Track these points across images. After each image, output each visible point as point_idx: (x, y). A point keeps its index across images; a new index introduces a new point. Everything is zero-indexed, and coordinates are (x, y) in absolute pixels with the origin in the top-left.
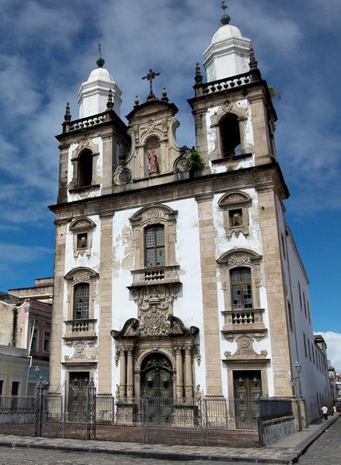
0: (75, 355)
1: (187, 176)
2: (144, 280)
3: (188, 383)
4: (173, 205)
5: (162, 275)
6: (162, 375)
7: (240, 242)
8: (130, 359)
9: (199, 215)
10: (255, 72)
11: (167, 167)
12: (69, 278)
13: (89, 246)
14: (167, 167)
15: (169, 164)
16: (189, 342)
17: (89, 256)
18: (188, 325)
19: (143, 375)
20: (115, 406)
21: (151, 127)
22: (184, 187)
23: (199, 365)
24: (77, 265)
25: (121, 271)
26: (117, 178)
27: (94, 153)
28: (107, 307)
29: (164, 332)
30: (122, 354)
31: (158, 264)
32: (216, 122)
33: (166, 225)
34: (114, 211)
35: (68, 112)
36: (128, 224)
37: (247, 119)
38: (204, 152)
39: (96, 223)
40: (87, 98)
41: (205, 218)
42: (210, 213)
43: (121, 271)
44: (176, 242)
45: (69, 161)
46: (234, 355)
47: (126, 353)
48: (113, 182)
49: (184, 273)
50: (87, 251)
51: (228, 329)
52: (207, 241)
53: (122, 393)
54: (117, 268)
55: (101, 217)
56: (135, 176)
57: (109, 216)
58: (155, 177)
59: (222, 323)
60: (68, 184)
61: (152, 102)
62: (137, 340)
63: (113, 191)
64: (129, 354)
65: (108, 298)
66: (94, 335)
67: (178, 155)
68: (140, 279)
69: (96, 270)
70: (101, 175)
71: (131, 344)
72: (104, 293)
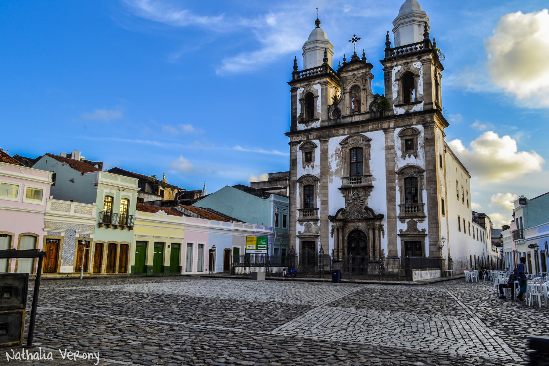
0: (305, 231)
1: (378, 115)
2: (349, 184)
3: (377, 247)
4: (368, 135)
5: (361, 181)
6: (361, 244)
7: (411, 161)
8: (340, 234)
10: (426, 41)
11: (365, 108)
13: (313, 161)
14: (365, 108)
15: (367, 106)
16: (377, 223)
17: (313, 167)
18: (377, 213)
19: (349, 243)
20: (331, 262)
21: (354, 79)
22: (375, 123)
23: (383, 237)
24: (305, 173)
25: (334, 177)
26: (331, 114)
27: (315, 96)
28: (325, 201)
29: (361, 217)
30: (336, 230)
31: (359, 173)
32: (398, 77)
33: (364, 148)
34: (329, 137)
35: (295, 63)
36: (340, 147)
37: (420, 76)
38: (390, 98)
39: (317, 145)
40: (309, 53)
41: (390, 144)
42: (392, 141)
43: (334, 177)
44: (370, 159)
45: (298, 100)
46: (406, 231)
47: (338, 230)
49: (375, 179)
50: (312, 164)
51: (402, 215)
52: (390, 159)
53: (335, 254)
54: (332, 175)
55: (320, 141)
56: (343, 113)
57: (326, 140)
58: (357, 115)
60: (298, 116)
61: (355, 60)
62: (345, 221)
63: (328, 123)
64: (340, 230)
65: (326, 195)
66: (317, 219)
67: (372, 100)
68: (346, 183)
69: (318, 177)
71: (341, 224)
72: (323, 192)
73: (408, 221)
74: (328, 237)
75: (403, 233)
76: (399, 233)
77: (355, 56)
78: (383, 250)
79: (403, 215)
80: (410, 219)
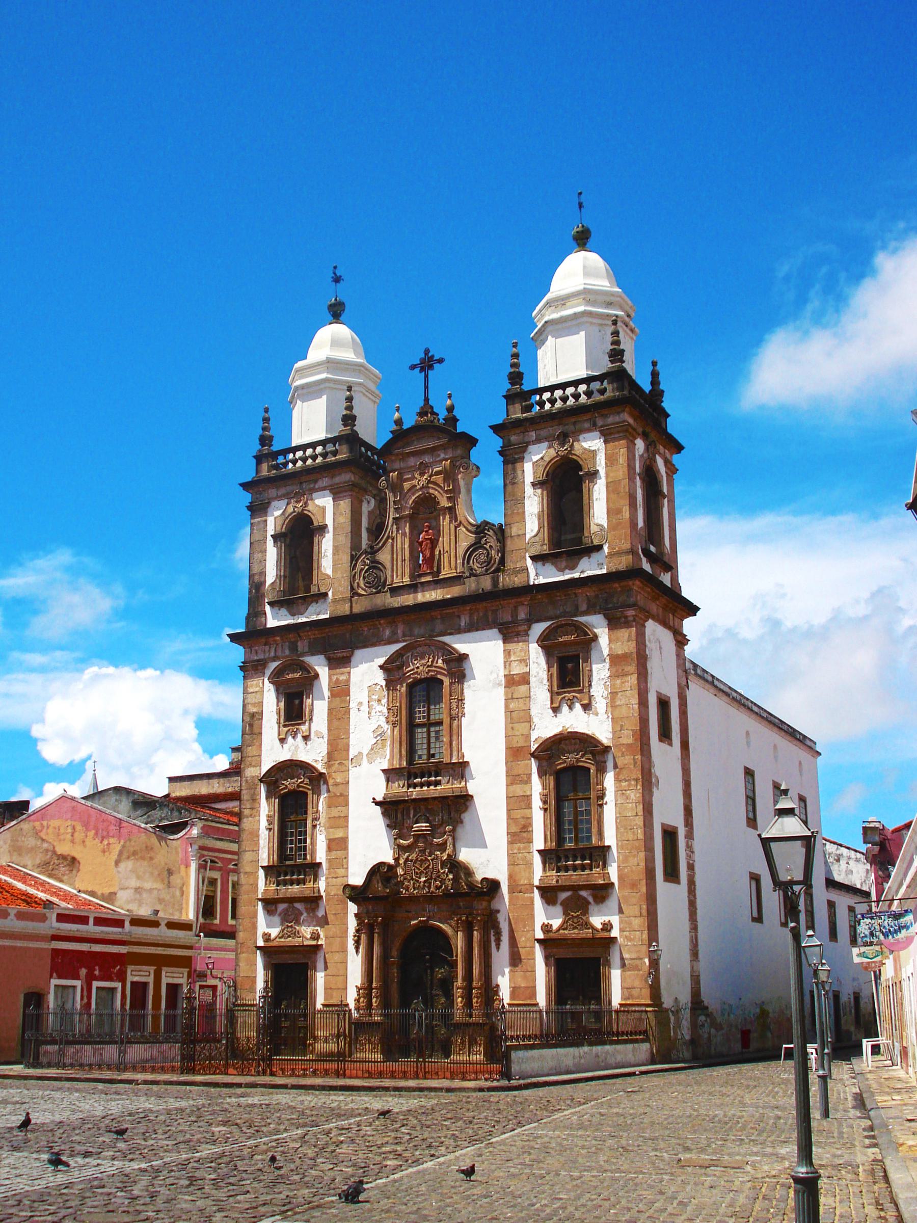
2: (405, 789)
9: (505, 662)
17: (306, 738)
24: (283, 754)
28: (342, 838)
29: (438, 888)
31: (433, 756)
41: (517, 669)
42: (525, 661)
46: (558, 930)
48: (352, 588)
50: (304, 728)
57: (344, 657)
65: (342, 821)
67: (472, 538)
68: (399, 788)
70: (329, 572)
72: (335, 812)
73: (567, 899)
74: (344, 951)
75: (551, 935)
76: (540, 935)
77: (426, 410)
79: (553, 878)
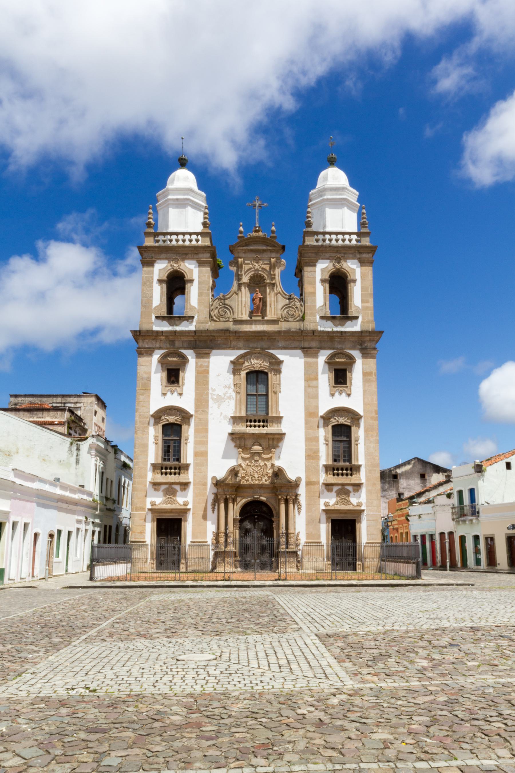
12: (157, 416)
44: (280, 392)
59: (323, 477)
78: (299, 532)
80: (340, 487)
